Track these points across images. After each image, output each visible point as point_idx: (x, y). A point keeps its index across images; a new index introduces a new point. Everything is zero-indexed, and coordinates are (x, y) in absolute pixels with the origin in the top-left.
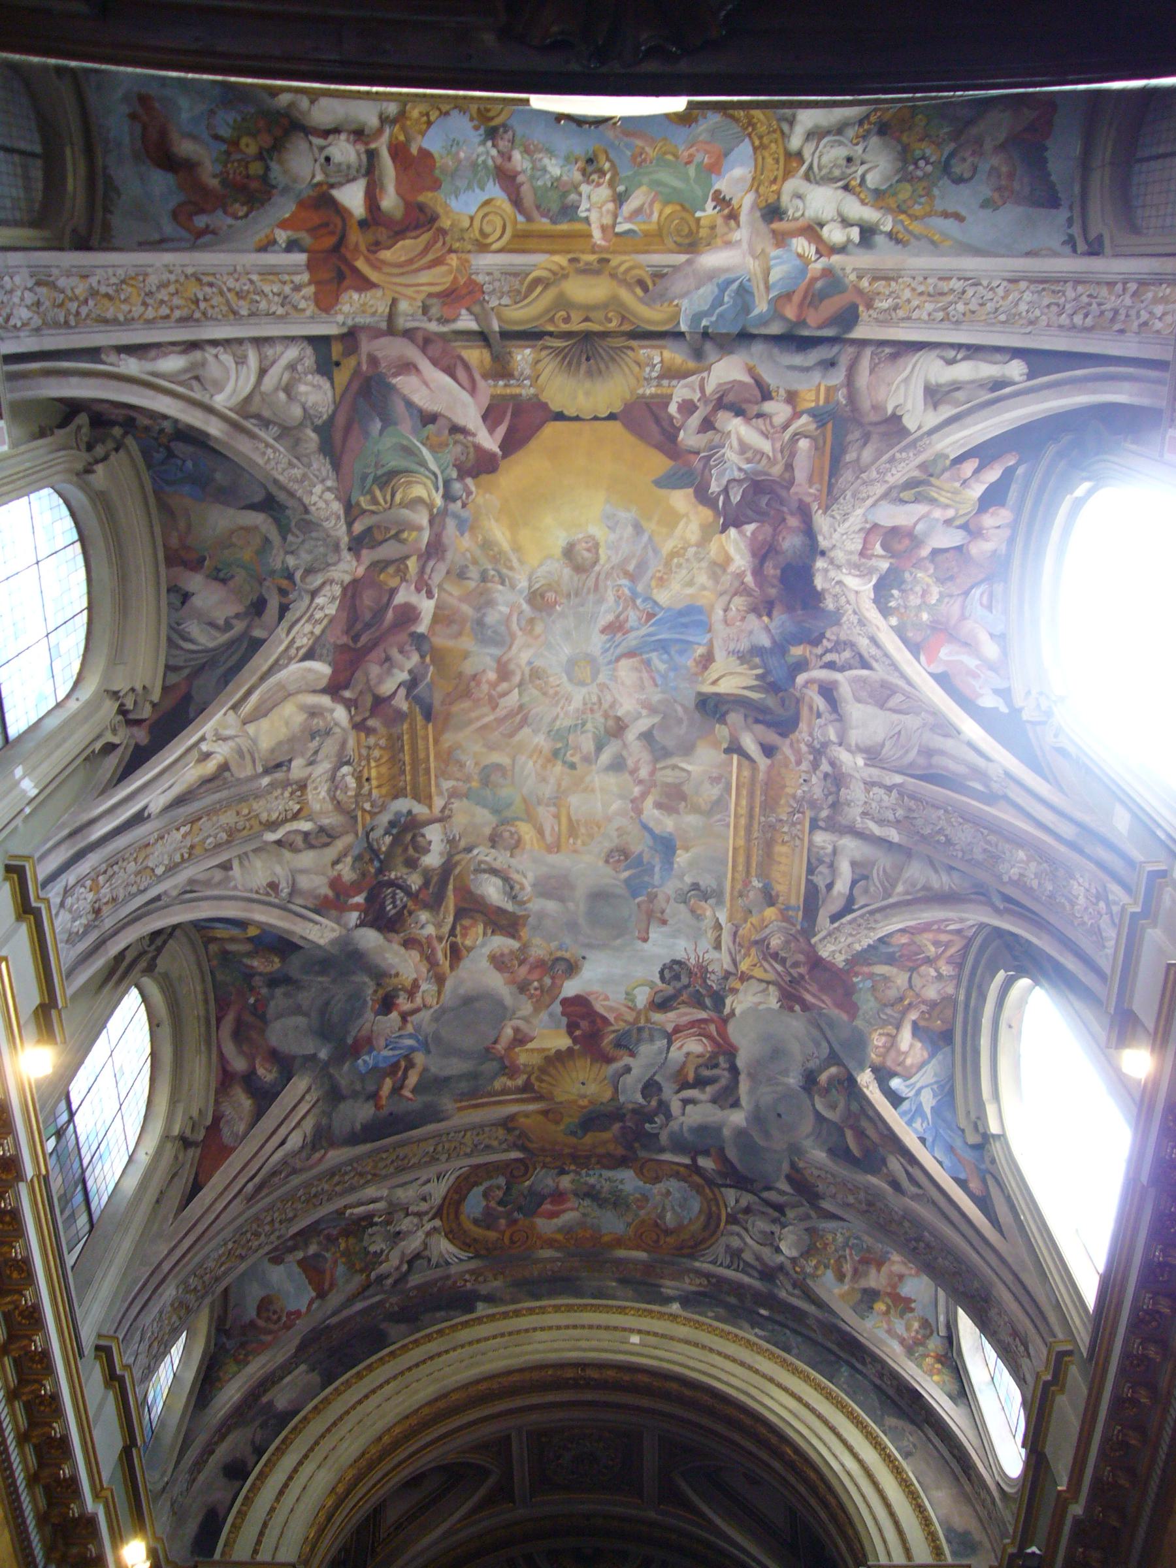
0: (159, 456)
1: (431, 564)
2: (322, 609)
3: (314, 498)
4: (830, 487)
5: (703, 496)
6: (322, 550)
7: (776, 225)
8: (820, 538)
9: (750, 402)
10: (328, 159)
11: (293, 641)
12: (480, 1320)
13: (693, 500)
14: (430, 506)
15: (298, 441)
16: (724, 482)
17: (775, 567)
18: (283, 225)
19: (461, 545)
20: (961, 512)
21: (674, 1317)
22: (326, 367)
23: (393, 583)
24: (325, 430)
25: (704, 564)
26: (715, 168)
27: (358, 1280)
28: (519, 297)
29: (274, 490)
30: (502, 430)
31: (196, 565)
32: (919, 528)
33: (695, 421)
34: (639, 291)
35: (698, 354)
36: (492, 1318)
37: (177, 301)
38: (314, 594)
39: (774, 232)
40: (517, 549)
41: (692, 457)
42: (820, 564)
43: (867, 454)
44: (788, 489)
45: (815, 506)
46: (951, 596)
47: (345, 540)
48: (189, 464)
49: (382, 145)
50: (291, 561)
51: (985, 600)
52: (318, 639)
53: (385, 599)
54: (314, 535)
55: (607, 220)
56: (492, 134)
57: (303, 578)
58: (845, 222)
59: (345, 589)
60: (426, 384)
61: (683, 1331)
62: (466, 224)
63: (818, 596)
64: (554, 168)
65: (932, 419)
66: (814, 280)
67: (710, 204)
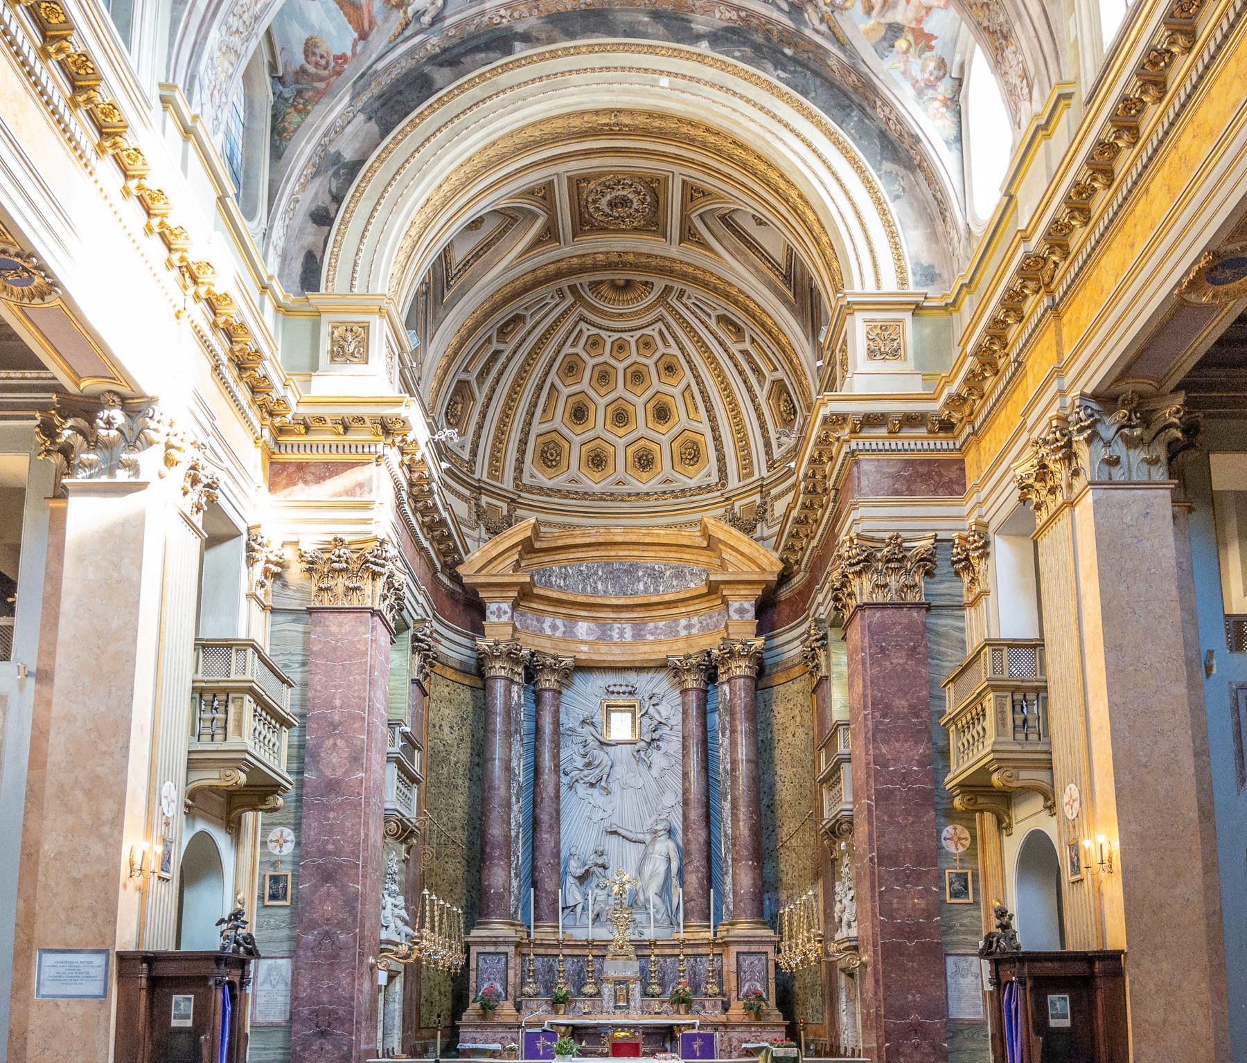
12: (518, 63)
21: (701, 58)
27: (398, 17)
36: (529, 60)
61: (710, 73)
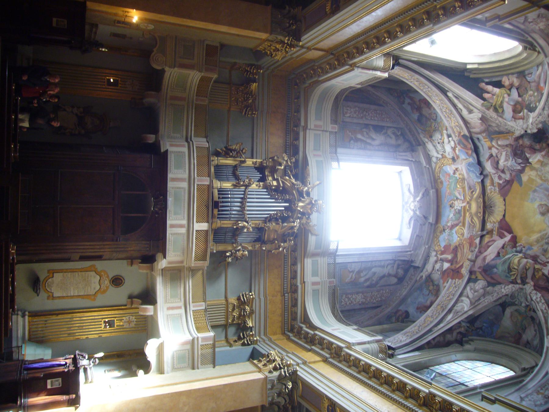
0: (481, 332)
1: (539, 260)
2: (537, 298)
3: (505, 292)
4: (507, 133)
5: (522, 171)
6: (522, 294)
7: (456, 158)
8: (522, 133)
9: (495, 160)
10: (438, 270)
11: (542, 310)
13: (524, 174)
14: (522, 258)
15: (488, 293)
16: (517, 165)
17: (537, 145)
18: (443, 283)
19: (536, 250)
20: (505, 92)
22: (476, 280)
23: (540, 273)
24: (490, 284)
25: (542, 168)
26: (449, 175)
28: (474, 226)
29: (498, 303)
30: (506, 233)
31: (520, 335)
32: (512, 103)
33: (503, 175)
34: (474, 193)
35: (486, 176)
37: (438, 311)
38: (532, 300)
39: (457, 159)
40: (540, 231)
41: (512, 176)
42: (529, 131)
43: (494, 125)
44: (512, 145)
45: (514, 136)
46: (530, 87)
47: (521, 286)
48: (485, 324)
49: (440, 257)
50: (523, 305)
51: (530, 76)
52: (546, 302)
53: (545, 277)
54: (516, 295)
55: (461, 202)
56: (444, 230)
57: (528, 302)
58: (449, 142)
59: (535, 289)
60: (489, 254)
62: (459, 238)
63: (539, 130)
64: (452, 215)
65: (475, 110)
66: (462, 147)
67: (456, 176)
